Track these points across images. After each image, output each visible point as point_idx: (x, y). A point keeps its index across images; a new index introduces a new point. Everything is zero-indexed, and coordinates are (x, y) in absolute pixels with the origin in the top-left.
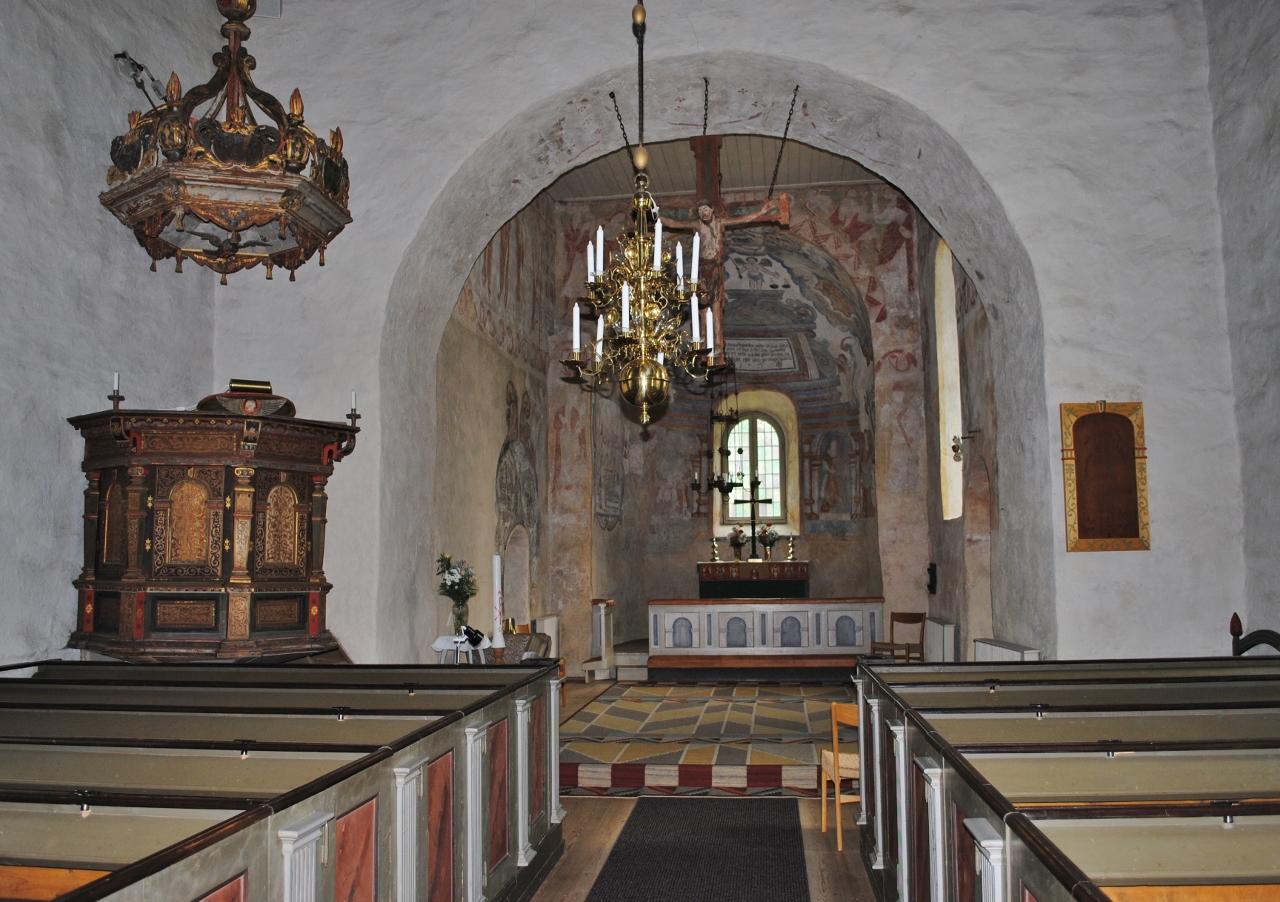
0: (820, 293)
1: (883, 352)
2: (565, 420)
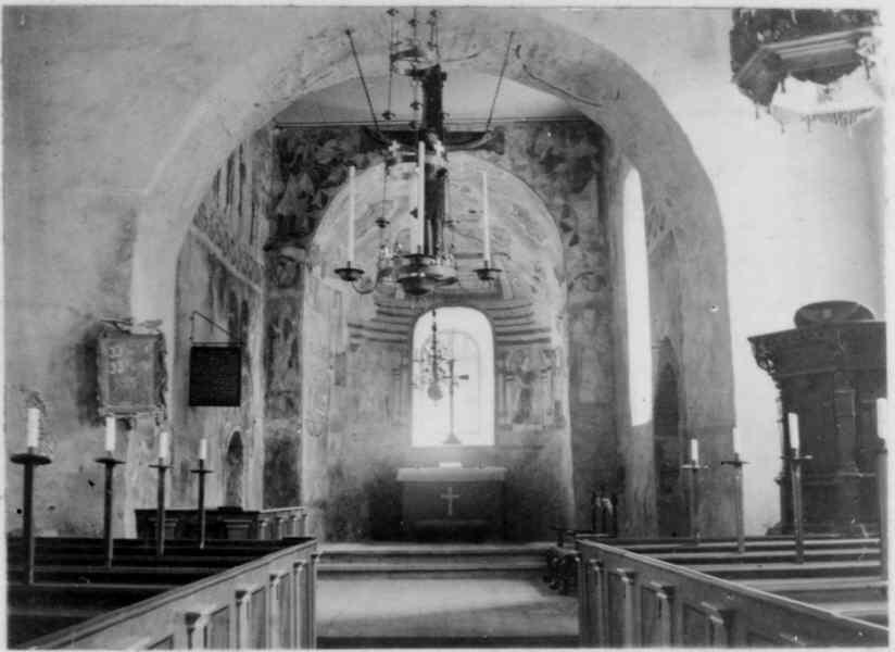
2: (279, 330)
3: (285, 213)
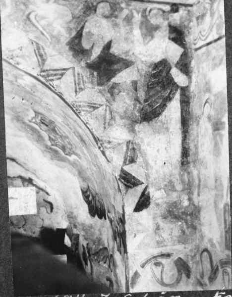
0: (37, 127)
1: (143, 258)
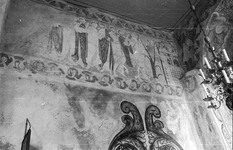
2: (198, 113)
3: (187, 60)
